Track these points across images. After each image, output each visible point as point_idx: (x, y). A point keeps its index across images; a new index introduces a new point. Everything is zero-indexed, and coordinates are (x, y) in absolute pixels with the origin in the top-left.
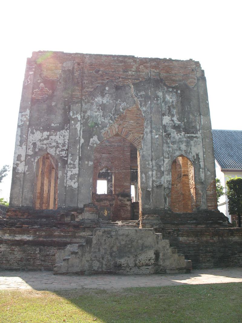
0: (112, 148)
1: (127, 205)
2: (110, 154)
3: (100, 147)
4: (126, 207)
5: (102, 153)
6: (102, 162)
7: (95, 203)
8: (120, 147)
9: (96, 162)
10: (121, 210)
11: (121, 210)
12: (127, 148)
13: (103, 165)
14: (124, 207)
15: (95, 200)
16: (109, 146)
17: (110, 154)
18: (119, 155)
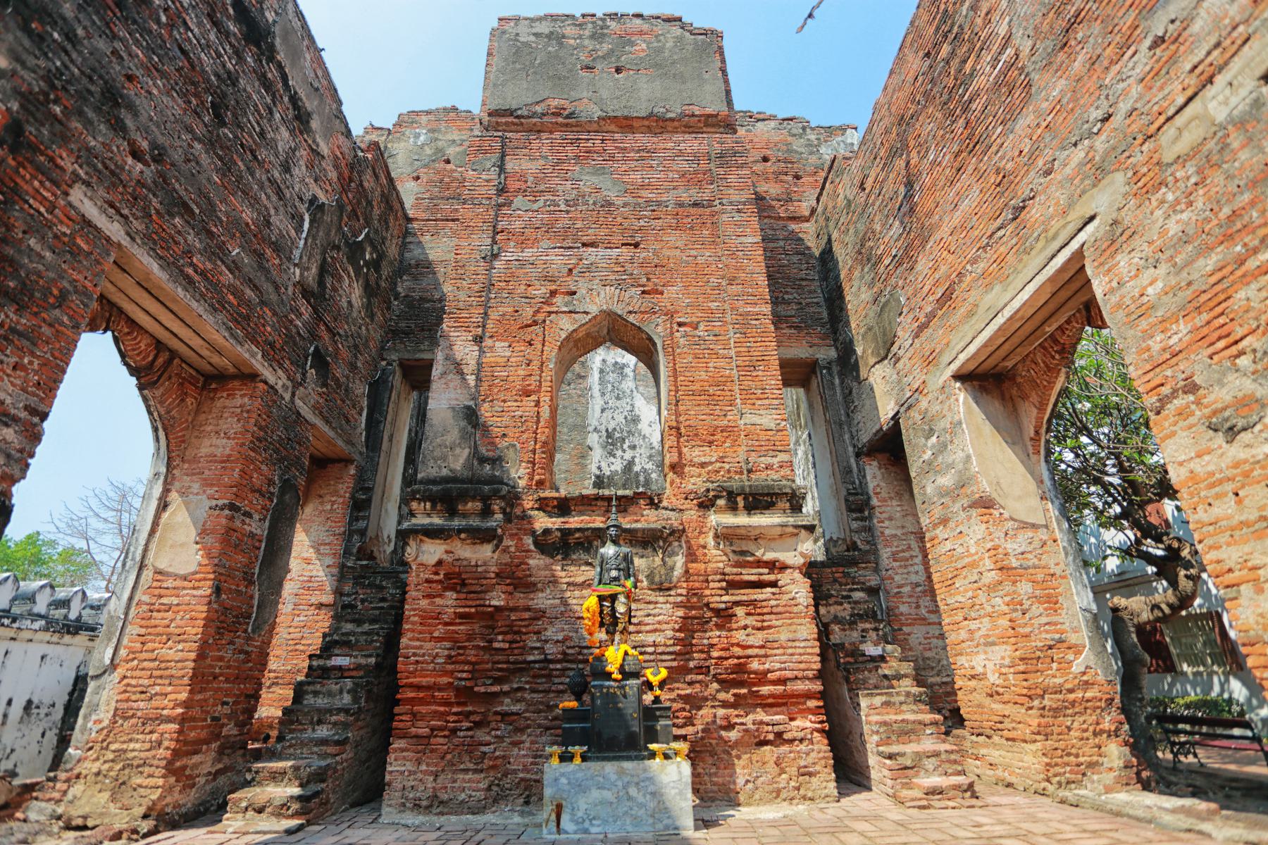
0: (646, 217)
1: (784, 567)
2: (636, 245)
3: (567, 212)
4: (774, 584)
5: (584, 245)
6: (582, 291)
7: (531, 562)
8: (693, 210)
9: (543, 290)
10: (740, 611)
11: (740, 611)
12: (739, 211)
13: (594, 309)
14: (760, 585)
15: (528, 541)
16: (625, 205)
17: (636, 245)
18: (693, 253)
